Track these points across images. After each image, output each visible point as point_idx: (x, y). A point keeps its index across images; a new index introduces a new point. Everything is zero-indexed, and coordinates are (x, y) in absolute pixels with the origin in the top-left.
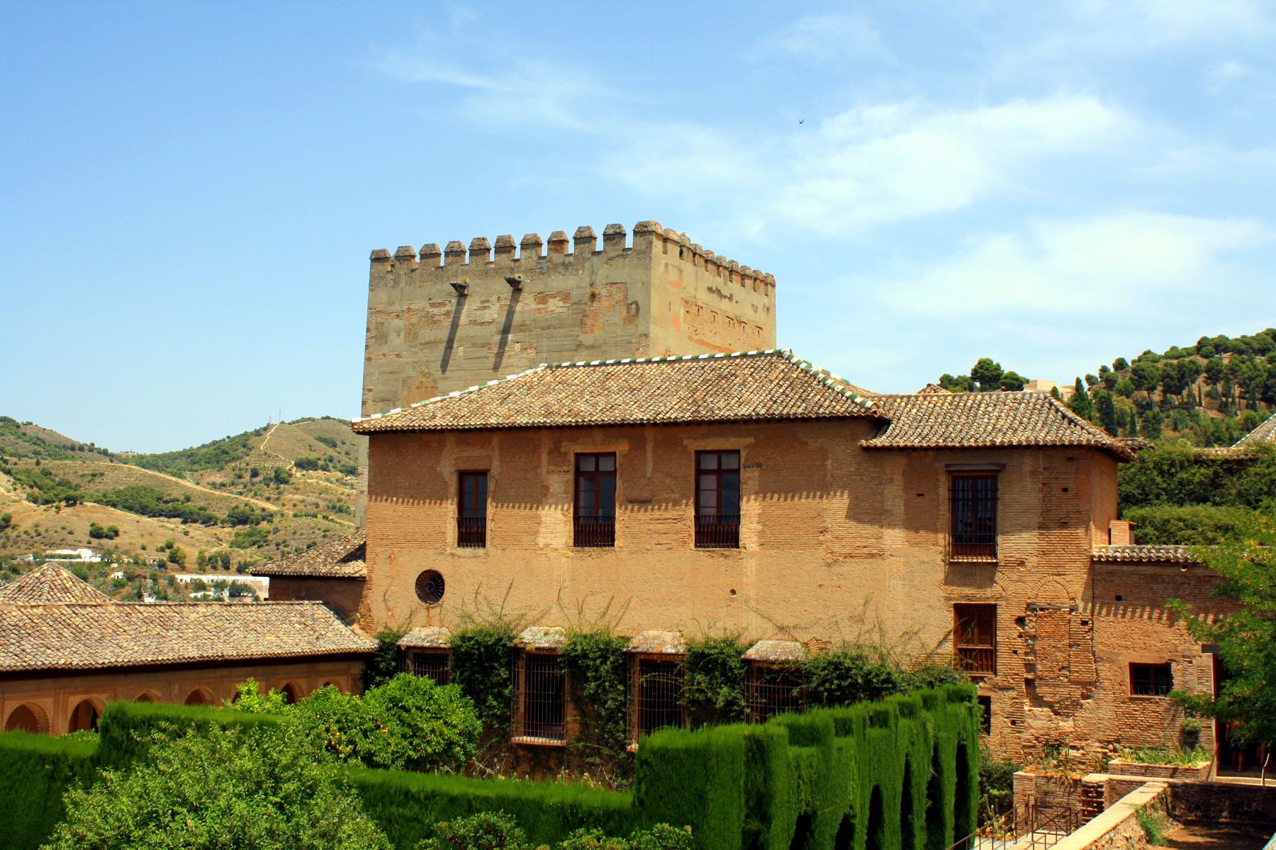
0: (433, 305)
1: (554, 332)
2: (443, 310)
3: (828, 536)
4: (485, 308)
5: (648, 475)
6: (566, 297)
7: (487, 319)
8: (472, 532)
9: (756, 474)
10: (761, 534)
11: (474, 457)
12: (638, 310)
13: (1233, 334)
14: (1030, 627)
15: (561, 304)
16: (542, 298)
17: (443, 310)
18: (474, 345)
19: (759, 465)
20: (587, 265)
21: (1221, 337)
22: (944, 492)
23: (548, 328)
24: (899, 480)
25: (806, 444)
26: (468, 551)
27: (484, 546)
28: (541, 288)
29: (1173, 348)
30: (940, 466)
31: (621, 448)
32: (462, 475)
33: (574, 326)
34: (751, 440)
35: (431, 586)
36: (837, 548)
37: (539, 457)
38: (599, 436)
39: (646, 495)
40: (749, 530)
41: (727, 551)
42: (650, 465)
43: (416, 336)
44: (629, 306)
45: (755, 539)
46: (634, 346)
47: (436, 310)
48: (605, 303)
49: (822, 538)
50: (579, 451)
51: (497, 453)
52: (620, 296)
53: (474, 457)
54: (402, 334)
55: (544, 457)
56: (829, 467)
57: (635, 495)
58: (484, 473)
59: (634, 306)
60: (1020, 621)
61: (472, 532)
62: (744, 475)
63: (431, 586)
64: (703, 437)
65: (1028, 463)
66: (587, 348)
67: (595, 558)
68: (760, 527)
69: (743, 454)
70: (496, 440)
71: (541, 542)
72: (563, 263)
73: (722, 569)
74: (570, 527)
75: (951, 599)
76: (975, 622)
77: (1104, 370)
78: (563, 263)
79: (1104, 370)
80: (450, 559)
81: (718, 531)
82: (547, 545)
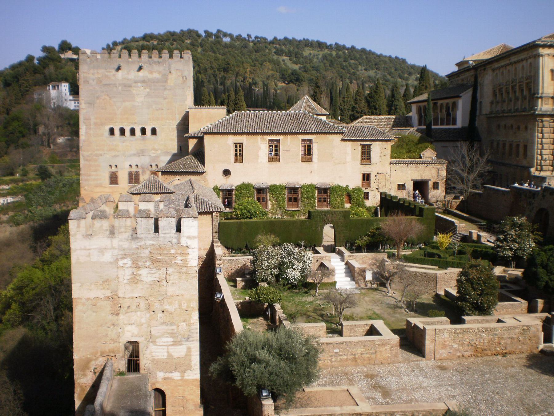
0: (107, 72)
5: (289, 144)
6: (159, 73)
7: (130, 77)
13: (156, 33)
14: (378, 177)
16: (151, 73)
17: (112, 74)
18: (125, 86)
20: (167, 63)
21: (152, 33)
22: (360, 148)
23: (154, 82)
26: (238, 164)
30: (359, 143)
31: (281, 137)
35: (227, 173)
43: (101, 82)
44: (183, 78)
47: (109, 74)
52: (179, 74)
54: (95, 81)
57: (285, 149)
60: (376, 176)
65: (378, 143)
67: (274, 164)
71: (259, 161)
76: (366, 177)
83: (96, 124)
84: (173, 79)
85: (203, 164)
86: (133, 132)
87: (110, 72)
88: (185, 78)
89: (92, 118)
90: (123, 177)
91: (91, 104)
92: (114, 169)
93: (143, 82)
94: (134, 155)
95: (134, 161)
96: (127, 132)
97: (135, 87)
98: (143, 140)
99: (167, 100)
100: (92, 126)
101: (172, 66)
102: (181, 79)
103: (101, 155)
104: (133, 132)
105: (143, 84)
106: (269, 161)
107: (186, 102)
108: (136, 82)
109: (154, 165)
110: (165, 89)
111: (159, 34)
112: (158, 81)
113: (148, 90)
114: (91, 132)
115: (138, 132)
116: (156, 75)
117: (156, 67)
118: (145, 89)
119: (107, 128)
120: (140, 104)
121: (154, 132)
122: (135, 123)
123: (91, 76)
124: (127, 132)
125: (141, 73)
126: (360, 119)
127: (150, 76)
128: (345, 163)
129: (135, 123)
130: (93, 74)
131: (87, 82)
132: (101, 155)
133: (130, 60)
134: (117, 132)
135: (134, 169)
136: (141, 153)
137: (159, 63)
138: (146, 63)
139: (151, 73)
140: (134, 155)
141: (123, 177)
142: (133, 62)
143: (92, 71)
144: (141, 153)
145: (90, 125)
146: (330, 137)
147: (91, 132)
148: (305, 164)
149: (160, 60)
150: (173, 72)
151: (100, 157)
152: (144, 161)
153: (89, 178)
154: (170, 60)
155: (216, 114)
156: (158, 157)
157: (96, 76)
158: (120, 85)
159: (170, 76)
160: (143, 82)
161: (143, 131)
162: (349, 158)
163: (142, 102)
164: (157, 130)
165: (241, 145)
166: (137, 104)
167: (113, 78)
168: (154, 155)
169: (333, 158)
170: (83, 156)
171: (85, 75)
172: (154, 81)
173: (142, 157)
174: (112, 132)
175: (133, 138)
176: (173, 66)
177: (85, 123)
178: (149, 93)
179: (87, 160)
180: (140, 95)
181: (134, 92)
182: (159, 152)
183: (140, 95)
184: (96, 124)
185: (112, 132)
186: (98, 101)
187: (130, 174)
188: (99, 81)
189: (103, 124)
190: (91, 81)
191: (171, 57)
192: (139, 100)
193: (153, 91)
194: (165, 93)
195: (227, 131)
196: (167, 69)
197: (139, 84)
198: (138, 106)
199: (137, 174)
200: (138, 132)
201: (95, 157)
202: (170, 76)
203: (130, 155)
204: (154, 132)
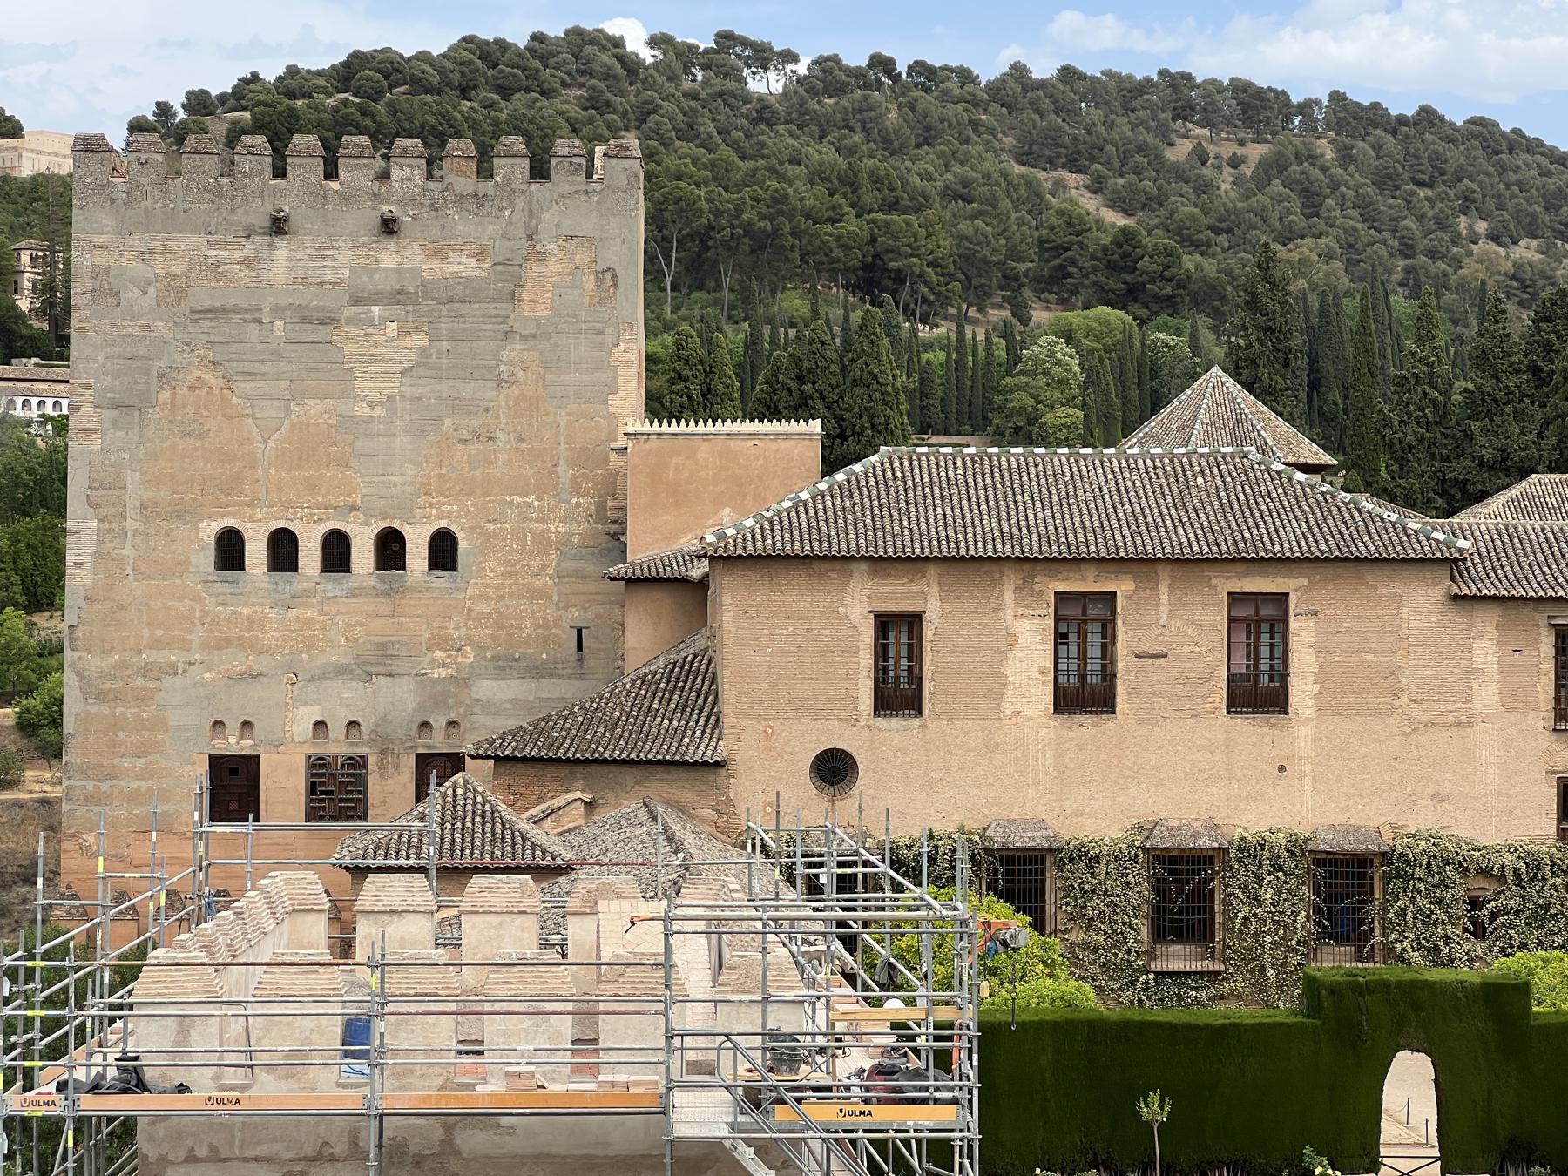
0: (212, 245)
1: (464, 309)
2: (237, 255)
3: (1405, 700)
4: (324, 258)
6: (480, 254)
7: (329, 276)
8: (898, 695)
9: (1311, 624)
10: (1317, 697)
11: (898, 594)
12: (615, 282)
15: (473, 262)
16: (439, 254)
17: (237, 255)
19: (1314, 613)
20: (520, 203)
21: (387, 50)
23: (450, 301)
24: (1491, 632)
25: (1376, 587)
27: (919, 713)
28: (434, 232)
29: (292, 71)
30: (1541, 618)
31: (1122, 587)
32: (885, 623)
33: (495, 300)
34: (1305, 582)
35: (834, 769)
36: (1416, 713)
37: (1001, 595)
38: (1091, 571)
39: (1158, 648)
40: (1301, 690)
41: (1273, 719)
42: (1164, 609)
43: (181, 294)
45: (1311, 702)
46: (609, 339)
48: (555, 267)
49: (1396, 702)
50: (1062, 588)
51: (935, 589)
52: (582, 258)
53: (898, 594)
54: (152, 291)
55: (1009, 595)
56: (1405, 616)
57: (1144, 648)
58: (913, 621)
59: (609, 275)
61: (898, 695)
62: (1294, 624)
63: (834, 769)
64: (1239, 576)
66: (524, 338)
67: (1086, 727)
68: (1316, 689)
69: (1293, 600)
70: (932, 571)
71: (1008, 709)
72: (475, 196)
73: (1268, 739)
74: (1049, 690)
75: (1554, 772)
77: (164, 110)
78: (475, 196)
79: (164, 110)
80: (865, 734)
81: (1258, 692)
82: (1017, 713)
83: (148, 510)
84: (551, 282)
85: (715, 722)
86: (336, 552)
87: (228, 246)
88: (608, 277)
89: (132, 478)
90: (283, 784)
91: (125, 407)
92: (233, 745)
93: (398, 296)
94: (342, 671)
95: (343, 701)
96: (310, 555)
97: (351, 322)
98: (387, 594)
99: (514, 392)
100: (131, 525)
101: (547, 215)
102: (590, 283)
103: (173, 671)
104: (336, 552)
105: (398, 310)
106: (1058, 709)
107: (613, 402)
108: (357, 301)
109: (439, 722)
110: (508, 335)
111: (423, 56)
112: (473, 292)
113: (420, 340)
114: (128, 551)
115: (363, 554)
116: (462, 265)
117: (463, 224)
118: (402, 333)
119: (209, 531)
120: (379, 412)
121: (444, 551)
122: (353, 508)
123: (129, 262)
124: (310, 555)
125: (389, 258)
126: (1513, 492)
127: (433, 269)
128: (1465, 723)
129: (353, 508)
130: (142, 257)
131: (107, 294)
132: (173, 671)
133: (335, 185)
134: (256, 553)
135: (336, 746)
136: (376, 663)
137: (479, 199)
138: (413, 202)
139: (439, 254)
140: (342, 671)
141: (283, 784)
142: (349, 198)
143: (136, 241)
144: (376, 663)
145: (123, 517)
146: (1386, 585)
147: (128, 551)
148: (1250, 729)
149: (488, 187)
150: (552, 248)
151: (168, 681)
152: (396, 700)
153: (105, 787)
154: (534, 187)
155: (766, 465)
156: (462, 681)
157: (158, 265)
158: (276, 309)
159: (534, 270)
160: (398, 296)
161: (390, 549)
162: (1486, 698)
163: (391, 398)
164: (462, 545)
165: (913, 621)
166: (361, 410)
167: (245, 277)
168: (445, 673)
169: (1397, 694)
170: (79, 674)
171: (101, 259)
172: (455, 296)
173: (382, 681)
174: (230, 550)
175: (334, 584)
176: (550, 216)
177: (94, 506)
178: (422, 352)
179: (103, 697)
180: (381, 358)
181: (349, 348)
182: (468, 657)
183: (381, 358)
184: (148, 510)
185: (230, 550)
186: (165, 395)
187: (318, 769)
188: (172, 290)
189: (185, 513)
190: (132, 293)
191: (539, 172)
192: (375, 388)
193: (445, 345)
194: (504, 356)
195: (839, 546)
196: (519, 232)
197: (376, 309)
198: (370, 420)
199: (356, 765)
200: (363, 554)
201: (140, 682)
202: (534, 270)
203: (306, 672)
204: (444, 551)
